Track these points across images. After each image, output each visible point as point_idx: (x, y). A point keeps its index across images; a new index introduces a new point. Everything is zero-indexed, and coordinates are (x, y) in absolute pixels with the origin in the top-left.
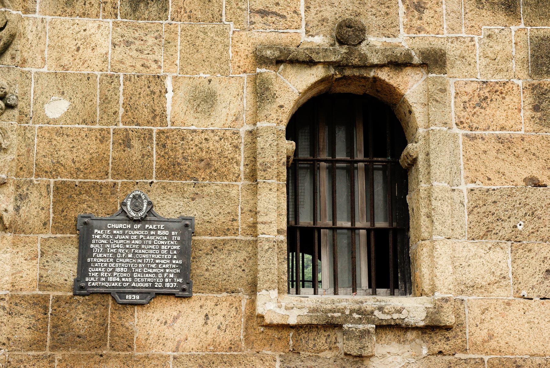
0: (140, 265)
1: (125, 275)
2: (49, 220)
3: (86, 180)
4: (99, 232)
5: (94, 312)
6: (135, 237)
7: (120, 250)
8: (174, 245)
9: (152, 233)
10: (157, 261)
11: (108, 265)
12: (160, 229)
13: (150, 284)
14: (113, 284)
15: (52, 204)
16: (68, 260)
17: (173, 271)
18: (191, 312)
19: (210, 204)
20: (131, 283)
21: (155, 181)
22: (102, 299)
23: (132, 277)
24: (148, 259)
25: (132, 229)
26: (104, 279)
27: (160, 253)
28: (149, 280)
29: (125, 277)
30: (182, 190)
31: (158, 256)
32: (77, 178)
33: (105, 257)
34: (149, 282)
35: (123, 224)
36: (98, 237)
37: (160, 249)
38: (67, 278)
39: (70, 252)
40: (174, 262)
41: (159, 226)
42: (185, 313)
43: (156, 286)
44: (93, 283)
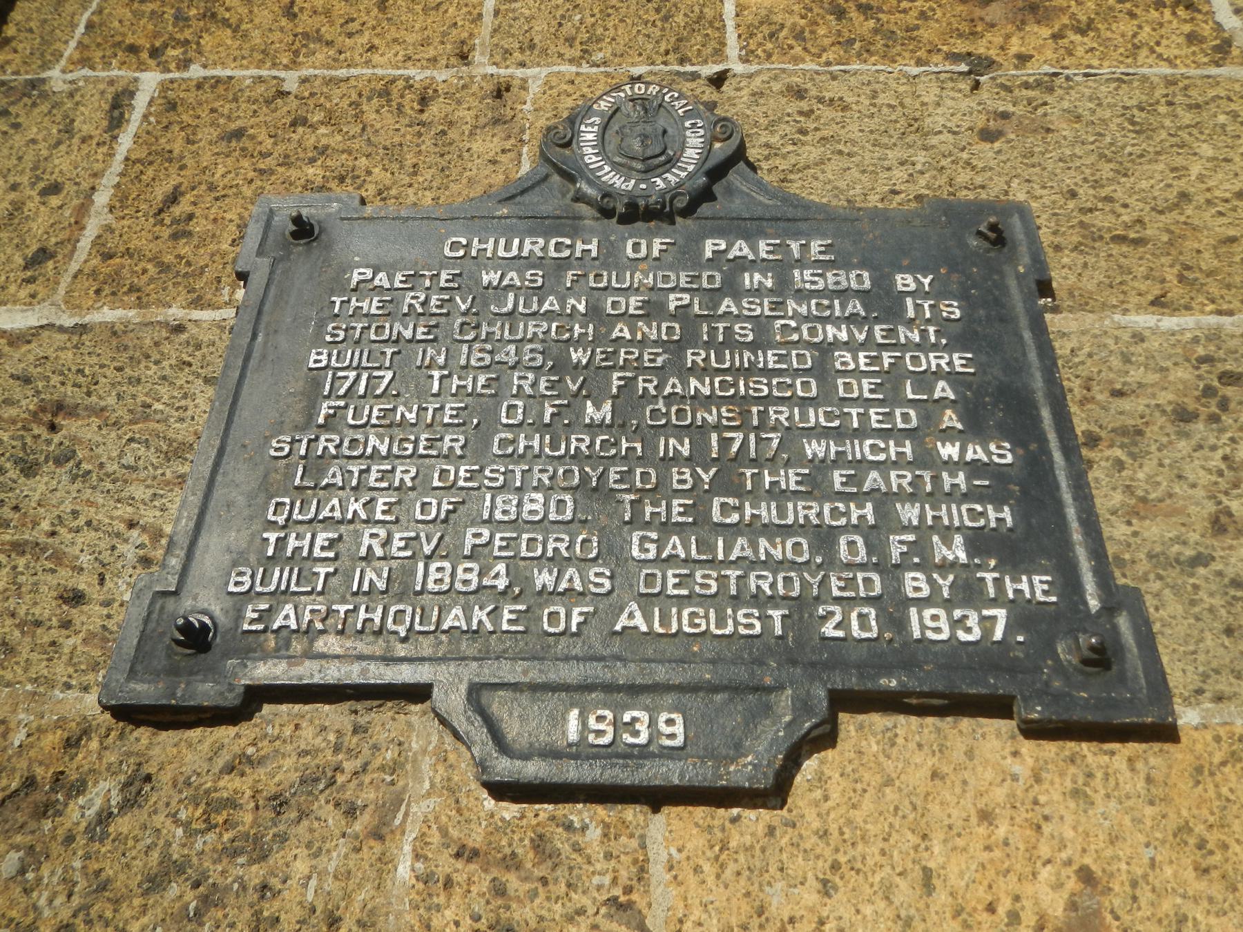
0: (681, 477)
1: (557, 544)
2: (73, 242)
3: (342, 73)
4: (382, 279)
5: (255, 874)
6: (634, 301)
7: (521, 381)
8: (923, 346)
9: (750, 280)
10: (814, 448)
11: (421, 483)
12: (801, 263)
13: (776, 614)
14: (457, 611)
15: (117, 165)
16: (129, 459)
17: (958, 514)
18: (1200, 886)
19: (1102, 156)
20: (610, 604)
21: (738, 68)
22: (352, 753)
23: (613, 553)
24: (738, 437)
25: (610, 257)
26: (374, 577)
27: (826, 396)
28: (759, 581)
29: (557, 562)
30: (907, 101)
31: (816, 417)
32: (294, 64)
33: (403, 422)
34: (758, 600)
35: (547, 235)
36: (372, 305)
37: (822, 370)
38: (83, 583)
39: (158, 406)
40: (949, 451)
41: (795, 246)
42: (1145, 895)
43: (829, 630)
44: (288, 609)
